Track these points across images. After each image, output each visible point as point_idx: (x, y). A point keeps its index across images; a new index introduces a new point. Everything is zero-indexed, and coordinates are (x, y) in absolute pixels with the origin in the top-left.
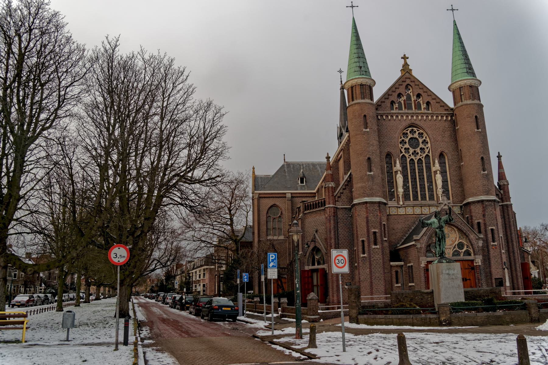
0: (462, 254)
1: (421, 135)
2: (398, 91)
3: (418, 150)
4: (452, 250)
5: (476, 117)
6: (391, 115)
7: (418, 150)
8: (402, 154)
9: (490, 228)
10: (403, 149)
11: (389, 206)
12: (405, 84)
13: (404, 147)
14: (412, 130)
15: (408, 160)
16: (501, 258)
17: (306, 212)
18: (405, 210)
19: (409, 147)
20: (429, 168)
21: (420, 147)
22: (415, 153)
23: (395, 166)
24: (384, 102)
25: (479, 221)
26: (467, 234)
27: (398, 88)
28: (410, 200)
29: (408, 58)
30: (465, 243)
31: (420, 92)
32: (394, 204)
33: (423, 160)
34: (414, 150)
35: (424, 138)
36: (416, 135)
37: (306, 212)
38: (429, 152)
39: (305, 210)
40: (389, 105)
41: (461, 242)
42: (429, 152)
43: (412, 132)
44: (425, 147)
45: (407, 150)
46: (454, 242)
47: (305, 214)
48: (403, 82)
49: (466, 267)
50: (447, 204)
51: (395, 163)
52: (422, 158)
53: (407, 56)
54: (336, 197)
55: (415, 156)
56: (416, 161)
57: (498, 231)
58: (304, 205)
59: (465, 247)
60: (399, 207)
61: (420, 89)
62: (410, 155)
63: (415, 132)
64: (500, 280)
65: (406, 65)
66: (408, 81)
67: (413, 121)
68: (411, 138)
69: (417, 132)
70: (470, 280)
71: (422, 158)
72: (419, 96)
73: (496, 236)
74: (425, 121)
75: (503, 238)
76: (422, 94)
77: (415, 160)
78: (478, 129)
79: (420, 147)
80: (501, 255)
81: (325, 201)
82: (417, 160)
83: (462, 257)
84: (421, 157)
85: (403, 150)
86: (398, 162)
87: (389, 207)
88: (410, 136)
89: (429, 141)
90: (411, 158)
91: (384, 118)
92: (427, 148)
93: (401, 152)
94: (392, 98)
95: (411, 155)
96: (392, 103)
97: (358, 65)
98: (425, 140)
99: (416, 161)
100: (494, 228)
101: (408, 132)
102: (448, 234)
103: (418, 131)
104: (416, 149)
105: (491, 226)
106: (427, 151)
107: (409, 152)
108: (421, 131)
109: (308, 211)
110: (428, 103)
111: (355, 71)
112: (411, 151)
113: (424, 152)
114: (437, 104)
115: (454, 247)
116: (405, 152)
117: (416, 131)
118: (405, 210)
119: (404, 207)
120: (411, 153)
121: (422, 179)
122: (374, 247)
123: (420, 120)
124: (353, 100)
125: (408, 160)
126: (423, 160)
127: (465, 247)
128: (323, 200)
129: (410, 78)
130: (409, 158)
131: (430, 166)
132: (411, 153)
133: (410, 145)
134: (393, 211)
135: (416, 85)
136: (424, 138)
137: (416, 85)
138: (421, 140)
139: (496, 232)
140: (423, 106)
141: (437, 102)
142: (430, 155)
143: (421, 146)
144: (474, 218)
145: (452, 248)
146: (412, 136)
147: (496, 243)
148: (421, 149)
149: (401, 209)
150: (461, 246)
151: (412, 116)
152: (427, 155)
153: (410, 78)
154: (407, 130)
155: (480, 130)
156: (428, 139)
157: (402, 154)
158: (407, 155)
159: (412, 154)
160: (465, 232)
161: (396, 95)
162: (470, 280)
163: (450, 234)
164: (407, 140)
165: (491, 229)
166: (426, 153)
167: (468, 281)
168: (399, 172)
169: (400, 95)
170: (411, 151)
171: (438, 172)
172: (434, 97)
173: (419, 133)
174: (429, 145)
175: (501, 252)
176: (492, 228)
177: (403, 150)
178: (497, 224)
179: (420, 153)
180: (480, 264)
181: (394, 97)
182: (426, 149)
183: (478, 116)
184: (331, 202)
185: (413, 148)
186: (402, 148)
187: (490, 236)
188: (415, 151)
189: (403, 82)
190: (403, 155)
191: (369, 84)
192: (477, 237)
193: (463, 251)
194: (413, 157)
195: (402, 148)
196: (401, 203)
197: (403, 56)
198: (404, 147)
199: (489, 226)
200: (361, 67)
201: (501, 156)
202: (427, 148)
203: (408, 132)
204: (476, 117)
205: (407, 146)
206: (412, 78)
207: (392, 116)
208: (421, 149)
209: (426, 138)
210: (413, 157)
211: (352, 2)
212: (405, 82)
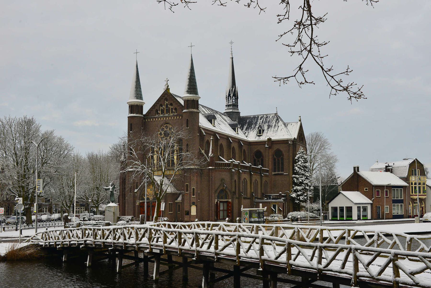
5: (187, 120)
6: (155, 118)
12: (164, 98)
16: (190, 200)
24: (152, 110)
31: (172, 102)
40: (154, 112)
43: (167, 127)
48: (163, 97)
57: (190, 186)
60: (155, 171)
64: (187, 212)
66: (166, 96)
73: (189, 188)
74: (173, 120)
78: (187, 127)
80: (190, 198)
94: (156, 108)
96: (157, 111)
123: (170, 120)
129: (167, 94)
135: (170, 98)
137: (170, 98)
139: (189, 186)
141: (180, 108)
147: (188, 192)
151: (166, 118)
153: (167, 94)
155: (188, 128)
161: (158, 105)
165: (187, 184)
175: (190, 197)
176: (187, 184)
178: (190, 182)
189: (163, 97)
204: (187, 120)
212: (164, 96)
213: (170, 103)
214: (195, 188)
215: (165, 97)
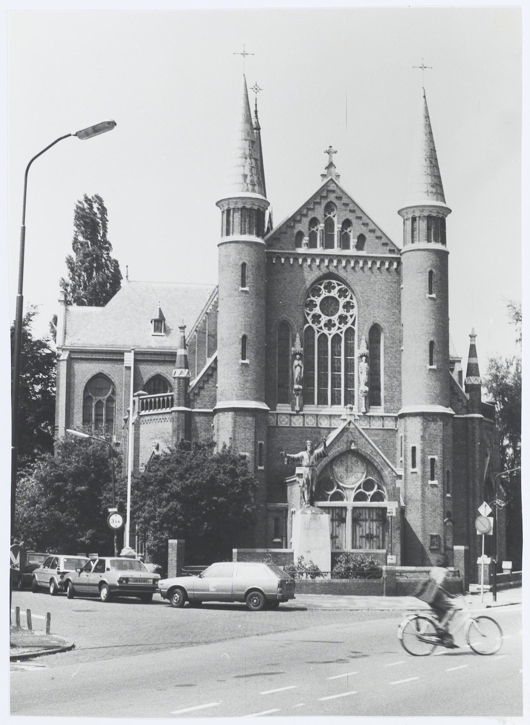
0: (369, 498)
1: (343, 293)
2: (311, 215)
3: (335, 318)
4: (354, 491)
7: (335, 318)
8: (307, 325)
9: (430, 457)
10: (310, 316)
11: (277, 412)
13: (312, 313)
14: (330, 283)
15: (317, 336)
17: (143, 413)
18: (304, 421)
19: (320, 313)
20: (349, 351)
21: (339, 313)
22: (329, 325)
23: (293, 346)
25: (414, 445)
26: (379, 468)
27: (313, 209)
28: (314, 404)
29: (335, 152)
30: (376, 481)
32: (284, 408)
33: (343, 336)
34: (328, 318)
35: (348, 299)
36: (334, 293)
37: (143, 413)
38: (353, 324)
39: (142, 409)
41: (369, 479)
42: (353, 324)
43: (330, 287)
44: (348, 314)
45: (316, 318)
46: (359, 480)
47: (142, 416)
50: (353, 421)
51: (294, 340)
52: (341, 333)
53: (334, 149)
54: (192, 395)
55: (329, 329)
56: (330, 338)
58: (141, 401)
59: (376, 487)
60: (294, 415)
61: (351, 211)
62: (321, 328)
63: (334, 288)
65: (331, 165)
66: (332, 197)
67: (332, 269)
68: (326, 298)
69: (338, 288)
70: (377, 537)
71: (341, 333)
72: (347, 223)
75: (451, 474)
76: (354, 221)
79: (339, 313)
81: (172, 400)
82: (332, 336)
83: (368, 503)
84: (338, 332)
85: (309, 318)
86: (298, 340)
87: (277, 414)
88: (324, 294)
89: (356, 305)
90: (322, 332)
91: (283, 262)
92: (351, 316)
93: (306, 322)
95: (323, 327)
97: (242, 173)
98: (348, 303)
99: (330, 338)
100: (436, 457)
101: (322, 287)
102: (352, 466)
103: (339, 285)
104: (332, 318)
105: (432, 455)
106: (350, 321)
107: (319, 322)
108: (343, 286)
109: (147, 412)
110: (361, 239)
111: (236, 183)
112: (324, 319)
113: (346, 323)
114: (377, 241)
115: (359, 487)
116: (313, 322)
117: (336, 285)
118: (304, 421)
119: (303, 415)
120: (322, 324)
121: (336, 368)
124: (228, 234)
125: (317, 336)
126: (343, 336)
127: (376, 487)
128: (170, 398)
130: (318, 332)
131: (353, 348)
132: (322, 324)
133: (322, 310)
134: (284, 422)
136: (348, 299)
138: (342, 301)
140: (353, 242)
141: (377, 238)
142: (356, 328)
143: (341, 311)
144: (408, 440)
145: (355, 489)
146: (328, 294)
148: (340, 317)
149: (297, 417)
150: (368, 485)
151: (331, 261)
152: (350, 328)
154: (321, 284)
156: (354, 301)
157: (307, 325)
158: (315, 327)
159: (325, 325)
160: (376, 464)
161: (306, 221)
162: (377, 537)
164: (318, 300)
166: (349, 325)
168: (298, 356)
169: (314, 222)
170: (324, 319)
171: (364, 358)
172: (372, 227)
173: (340, 291)
174: (354, 311)
177: (309, 318)
179: (338, 325)
180: (394, 514)
181: (303, 226)
182: (349, 318)
183: (434, 270)
184: (182, 401)
185: (328, 315)
186: (308, 314)
187: (428, 469)
188: (330, 321)
189: (322, 197)
190: (310, 326)
191: (256, 208)
192: (394, 474)
193: (371, 493)
194: (325, 331)
195: (308, 314)
196: (297, 408)
197: (328, 149)
198: (312, 313)
199: (429, 455)
200: (245, 176)
201: (475, 337)
202: (351, 316)
203: (322, 287)
205: (317, 310)
206: (338, 191)
207: (296, 259)
208: (340, 317)
209: (351, 298)
210: (325, 331)
211: (244, 45)
213: (345, 218)
214: (450, 469)
215: (329, 200)
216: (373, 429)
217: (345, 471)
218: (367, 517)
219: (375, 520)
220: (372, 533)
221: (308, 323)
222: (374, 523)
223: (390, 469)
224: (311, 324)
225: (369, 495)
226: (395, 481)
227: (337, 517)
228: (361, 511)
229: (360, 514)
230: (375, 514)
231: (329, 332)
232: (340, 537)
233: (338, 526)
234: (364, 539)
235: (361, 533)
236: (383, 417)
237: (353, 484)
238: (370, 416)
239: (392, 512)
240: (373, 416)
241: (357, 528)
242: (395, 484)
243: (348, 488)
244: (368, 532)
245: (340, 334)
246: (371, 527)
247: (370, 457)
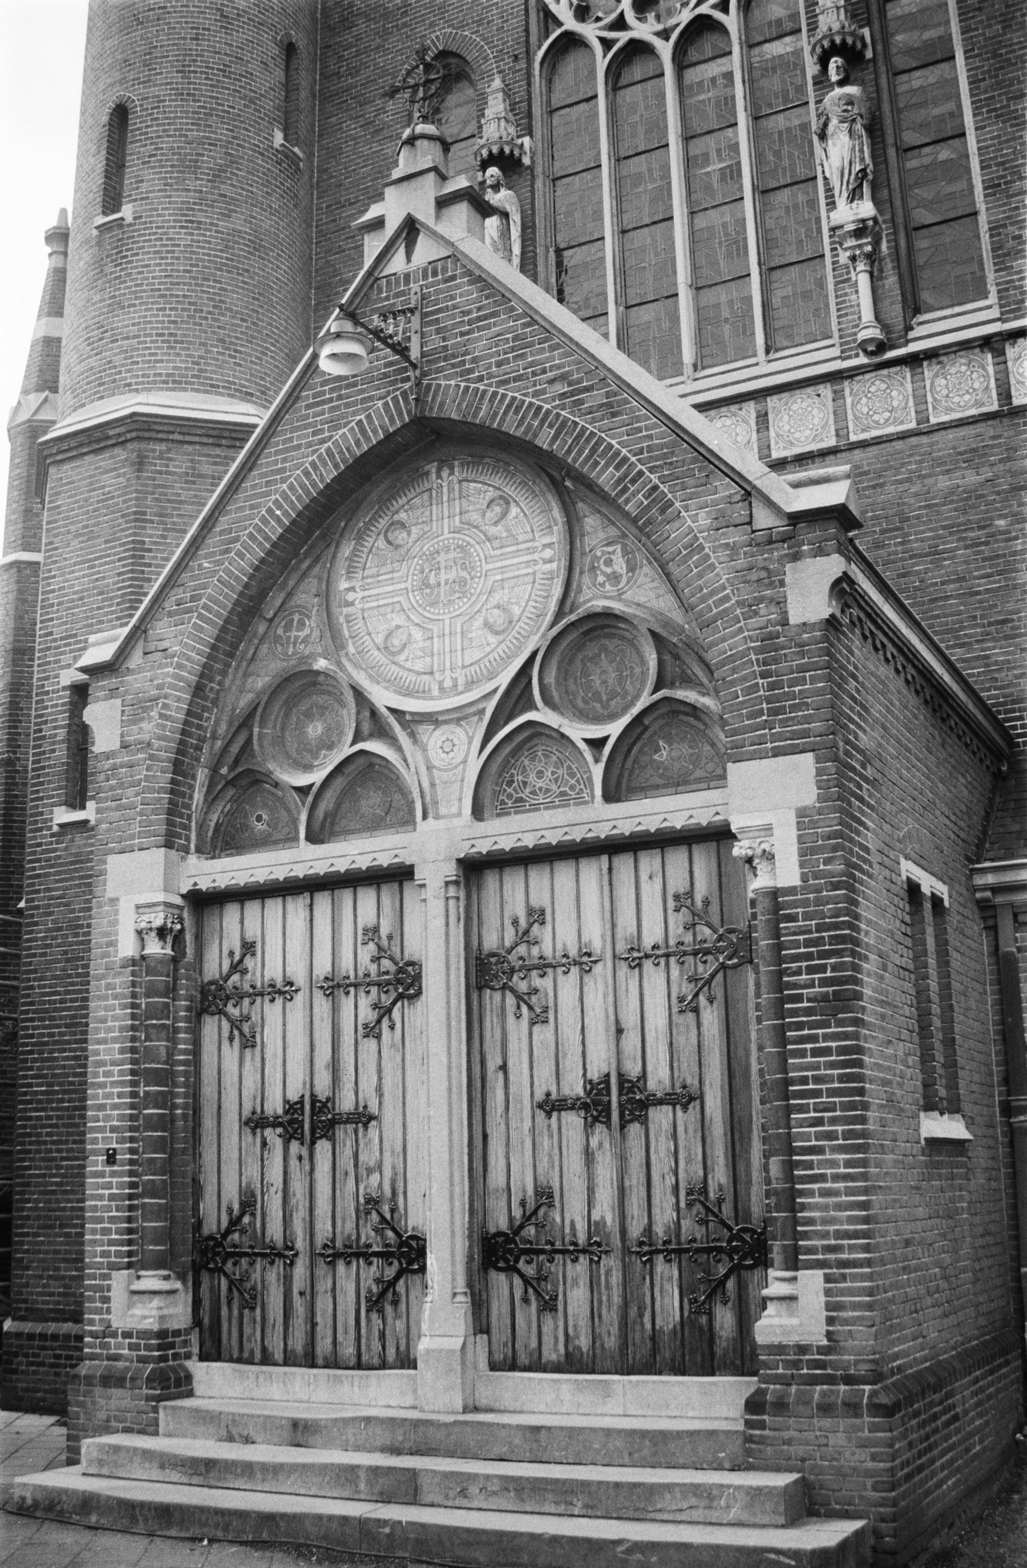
15: (602, 63)
49: (652, 935)
50: (425, 213)
56: (665, 50)
77: (658, 43)
90: (623, 37)
95: (630, 17)
122: (63, 816)
130: (607, 44)
163: (477, 551)
167: (660, 1117)
216: (943, 427)
217: (415, 598)
218: (595, 935)
219: (662, 954)
220: (633, 1069)
221: (560, 24)
222: (655, 978)
223: (725, 488)
224: (570, 23)
225: (597, 744)
226: (775, 580)
227: (366, 953)
228: (540, 898)
229: (537, 916)
230: (652, 891)
231: (660, 27)
232: (390, 1116)
233: (372, 1031)
234: (573, 1121)
235: (544, 1083)
236: (987, 343)
237: (470, 685)
238: (914, 361)
239: (769, 857)
240: (931, 355)
241: (518, 1030)
242: (781, 603)
243: (432, 719)
244: (600, 1063)
245: (718, 15)
246: (630, 1019)
247: (563, 427)
